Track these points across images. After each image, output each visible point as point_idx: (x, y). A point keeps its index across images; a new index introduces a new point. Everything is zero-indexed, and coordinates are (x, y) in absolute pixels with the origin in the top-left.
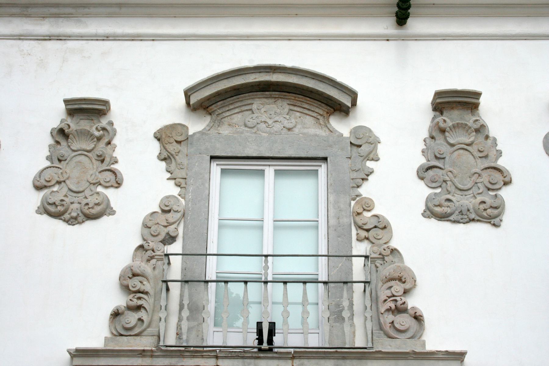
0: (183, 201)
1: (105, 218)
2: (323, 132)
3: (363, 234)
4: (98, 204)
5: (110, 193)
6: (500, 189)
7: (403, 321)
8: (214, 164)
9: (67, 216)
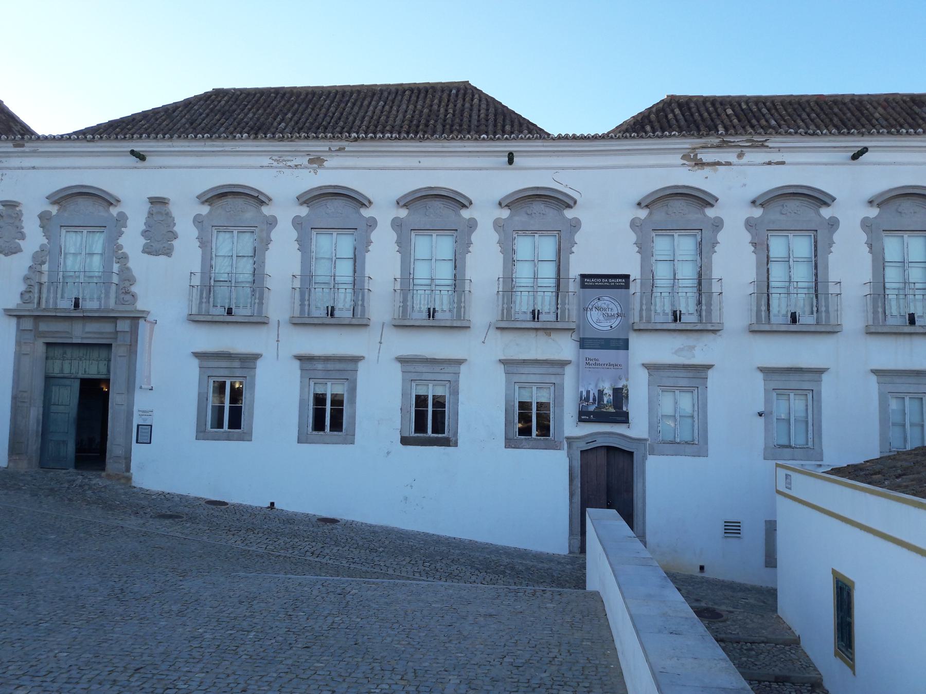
3: (117, 261)
4: (15, 248)
5: (21, 242)
7: (128, 297)
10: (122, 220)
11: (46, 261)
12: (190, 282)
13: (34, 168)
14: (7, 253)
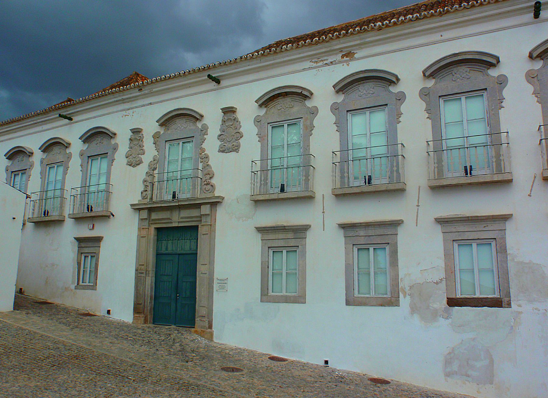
0: (158, 156)
2: (194, 128)
4: (139, 160)
5: (142, 156)
7: (209, 187)
9: (132, 165)
10: (204, 130)
12: (252, 169)
13: (151, 104)
14: (134, 165)
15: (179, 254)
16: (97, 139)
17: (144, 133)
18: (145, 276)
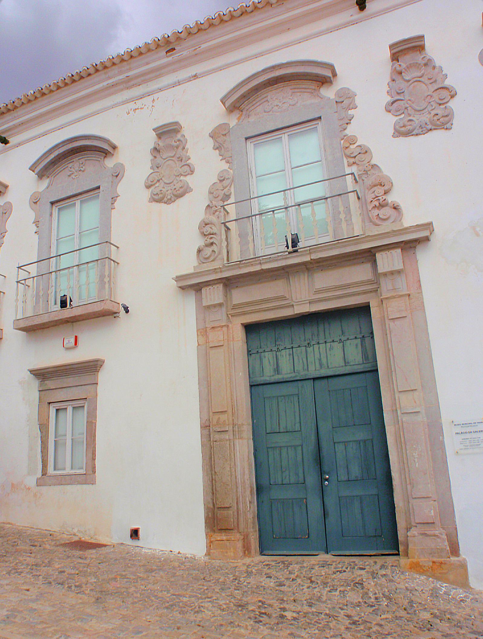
0: (231, 171)
1: (187, 195)
2: (316, 101)
3: (352, 160)
4: (181, 187)
5: (188, 179)
6: (448, 101)
7: (385, 212)
8: (248, 142)
9: (165, 199)
11: (230, 194)
13: (195, 77)
15: (314, 379)
16: (71, 165)
17: (186, 131)
18: (231, 437)
